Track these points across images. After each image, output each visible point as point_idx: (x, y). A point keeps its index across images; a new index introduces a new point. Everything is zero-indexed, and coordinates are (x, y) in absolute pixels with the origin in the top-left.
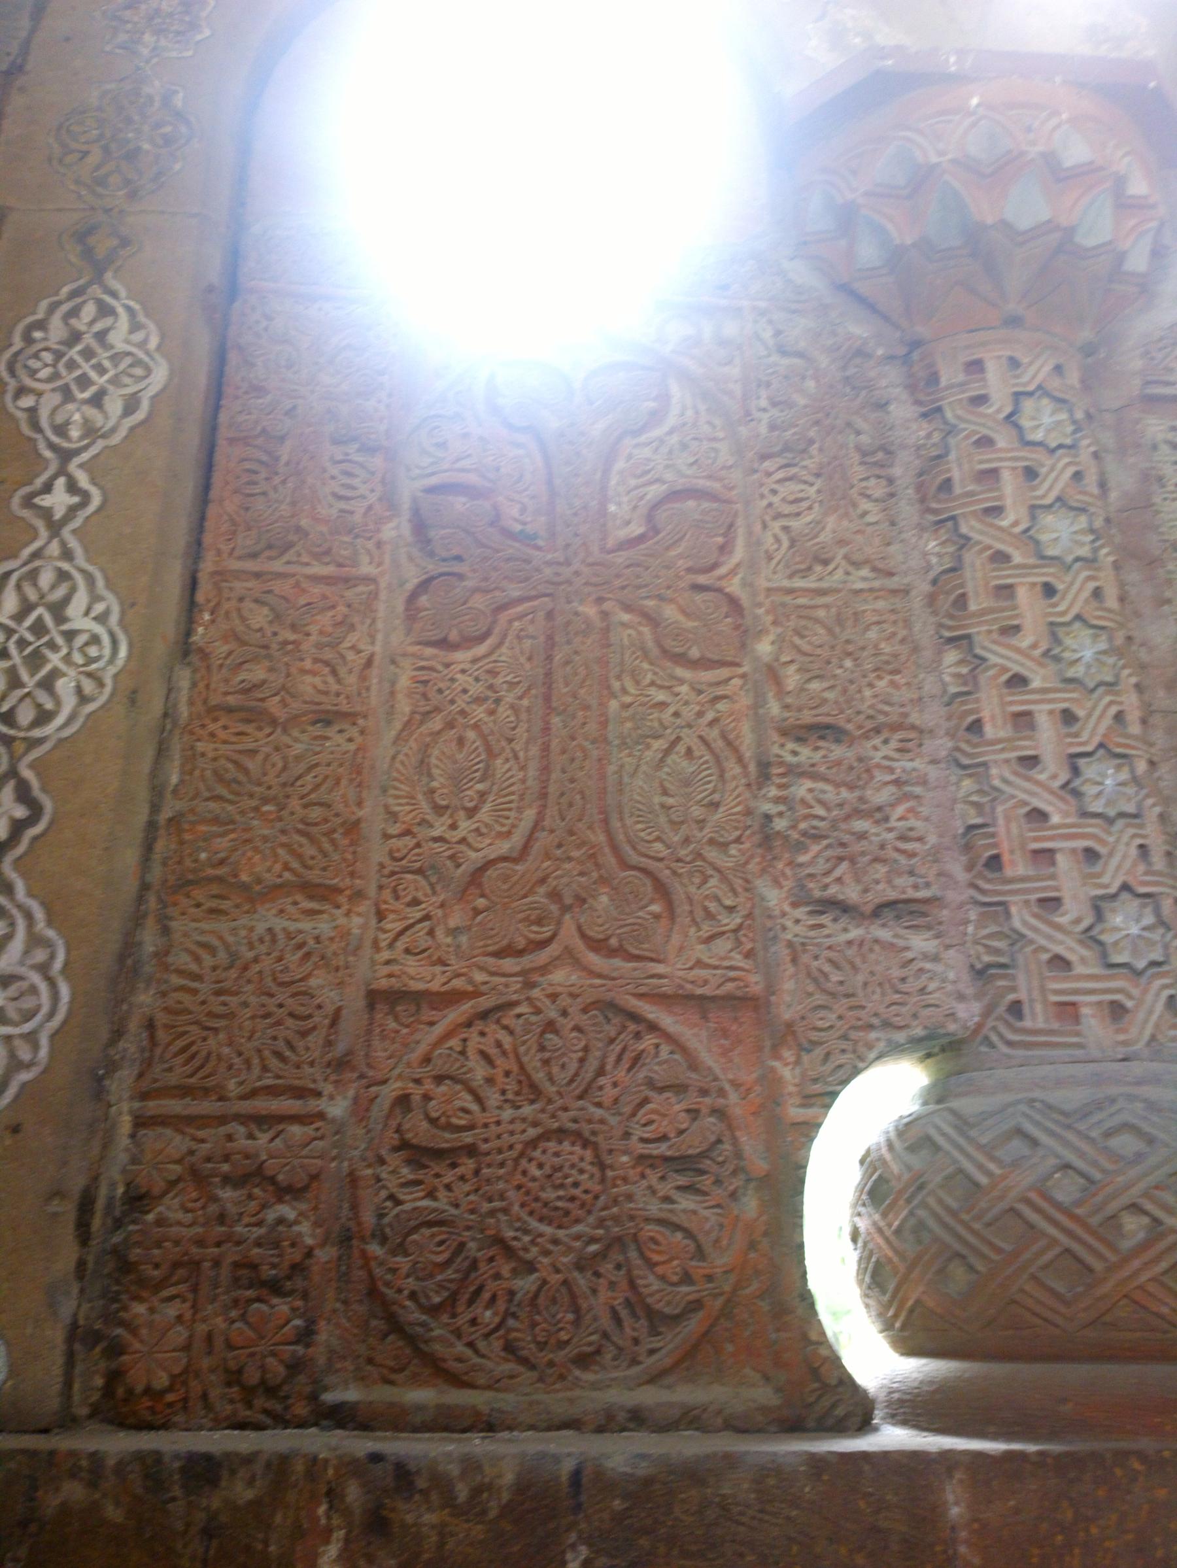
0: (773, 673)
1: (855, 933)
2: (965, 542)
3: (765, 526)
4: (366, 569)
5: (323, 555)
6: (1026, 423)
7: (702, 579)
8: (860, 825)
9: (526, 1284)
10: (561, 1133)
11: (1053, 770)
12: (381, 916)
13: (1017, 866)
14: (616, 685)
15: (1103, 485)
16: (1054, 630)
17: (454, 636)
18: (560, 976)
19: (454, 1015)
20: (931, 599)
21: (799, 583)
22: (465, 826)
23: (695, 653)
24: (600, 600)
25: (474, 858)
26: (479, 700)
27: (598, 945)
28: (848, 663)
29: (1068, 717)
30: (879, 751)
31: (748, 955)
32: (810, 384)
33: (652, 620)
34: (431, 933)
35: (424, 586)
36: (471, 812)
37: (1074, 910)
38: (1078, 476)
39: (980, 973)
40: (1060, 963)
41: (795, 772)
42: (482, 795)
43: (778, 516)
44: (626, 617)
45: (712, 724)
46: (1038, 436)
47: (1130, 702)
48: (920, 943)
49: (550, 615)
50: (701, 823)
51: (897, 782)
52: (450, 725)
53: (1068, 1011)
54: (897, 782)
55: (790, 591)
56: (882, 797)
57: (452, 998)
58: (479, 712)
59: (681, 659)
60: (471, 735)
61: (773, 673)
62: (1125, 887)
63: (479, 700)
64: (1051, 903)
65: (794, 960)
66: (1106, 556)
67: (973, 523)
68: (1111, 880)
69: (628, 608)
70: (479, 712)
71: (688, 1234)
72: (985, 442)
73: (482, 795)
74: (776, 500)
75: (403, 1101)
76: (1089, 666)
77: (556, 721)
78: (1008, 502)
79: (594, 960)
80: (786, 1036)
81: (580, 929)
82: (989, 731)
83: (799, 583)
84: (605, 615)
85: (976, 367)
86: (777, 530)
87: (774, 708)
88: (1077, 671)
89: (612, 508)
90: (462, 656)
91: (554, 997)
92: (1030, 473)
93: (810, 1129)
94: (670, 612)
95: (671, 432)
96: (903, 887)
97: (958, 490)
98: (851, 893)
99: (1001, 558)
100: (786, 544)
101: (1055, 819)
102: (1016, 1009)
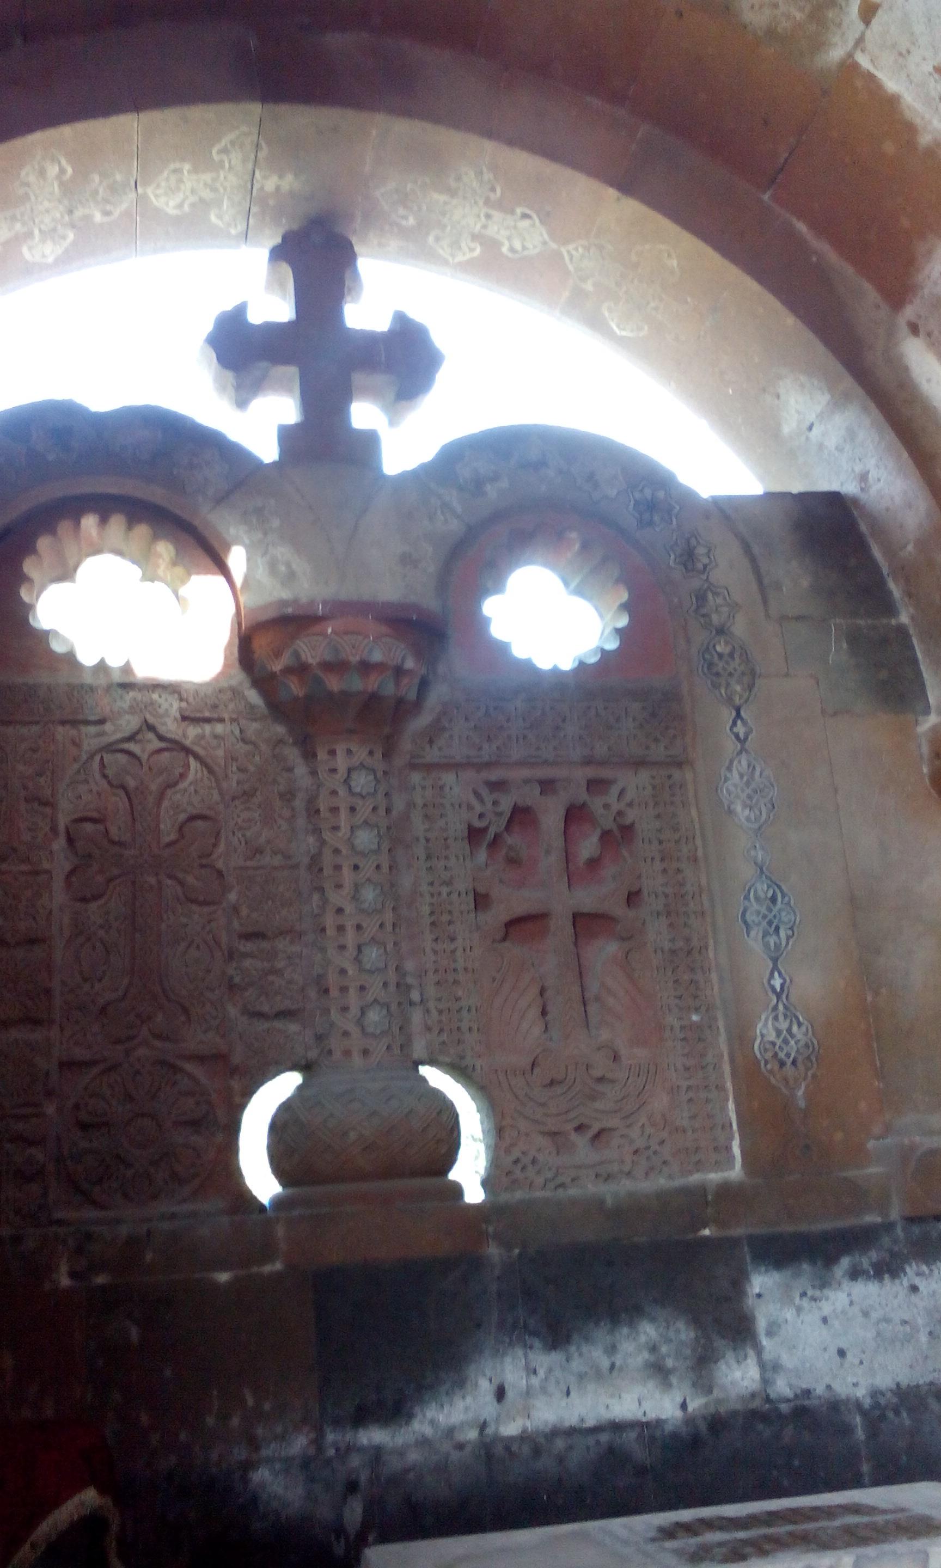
0: (236, 909)
1: (267, 1025)
2: (323, 843)
3: (234, 833)
4: (46, 865)
5: (27, 860)
6: (353, 784)
7: (204, 861)
8: (271, 978)
9: (129, 1173)
10: (143, 1115)
11: (351, 951)
12: (62, 1029)
13: (334, 993)
14: (165, 917)
15: (388, 811)
16: (357, 887)
17: (89, 896)
18: (142, 1052)
19: (95, 1071)
20: (310, 867)
21: (249, 863)
22: (97, 986)
23: (201, 898)
24: (157, 874)
25: (101, 1001)
26: (101, 927)
27: (159, 1037)
28: (270, 902)
29: (359, 927)
30: (282, 944)
31: (223, 1036)
32: (257, 758)
33: (182, 883)
34: (85, 1035)
35: (72, 872)
36: (100, 980)
37: (354, 1011)
38: (374, 809)
39: (319, 1038)
40: (346, 1034)
41: (246, 955)
42: (104, 972)
43: (240, 828)
44: (169, 882)
45: (208, 933)
46: (358, 790)
47: (389, 917)
48: (293, 1027)
49: (133, 883)
50: (203, 980)
51: (289, 958)
52: (89, 939)
53: (347, 1053)
54: (289, 958)
55: (247, 868)
56: (280, 964)
57: (93, 1063)
58: (101, 933)
59: (193, 901)
60: (98, 944)
61: (236, 909)
62: (376, 1001)
63: (101, 927)
64: (345, 1009)
65: (241, 1038)
66: (385, 846)
67: (329, 834)
68: (370, 997)
69: (170, 877)
70: (101, 933)
71: (194, 1149)
72: (334, 793)
73: (104, 972)
74: (240, 821)
75: (77, 1107)
76: (370, 904)
77: (138, 935)
78: (343, 824)
79: (157, 1043)
80: (234, 1071)
81: (149, 1030)
82: (328, 932)
83: (249, 863)
84: (159, 882)
85: (332, 753)
86: (240, 836)
87: (236, 924)
88: (366, 905)
89: (162, 826)
90: (93, 906)
91: (139, 1060)
92: (353, 809)
93: (242, 1107)
94: (190, 880)
95: (191, 784)
96: (287, 1004)
97: (322, 815)
98: (266, 1008)
99: (337, 851)
100: (243, 843)
101: (350, 972)
102: (330, 1052)
